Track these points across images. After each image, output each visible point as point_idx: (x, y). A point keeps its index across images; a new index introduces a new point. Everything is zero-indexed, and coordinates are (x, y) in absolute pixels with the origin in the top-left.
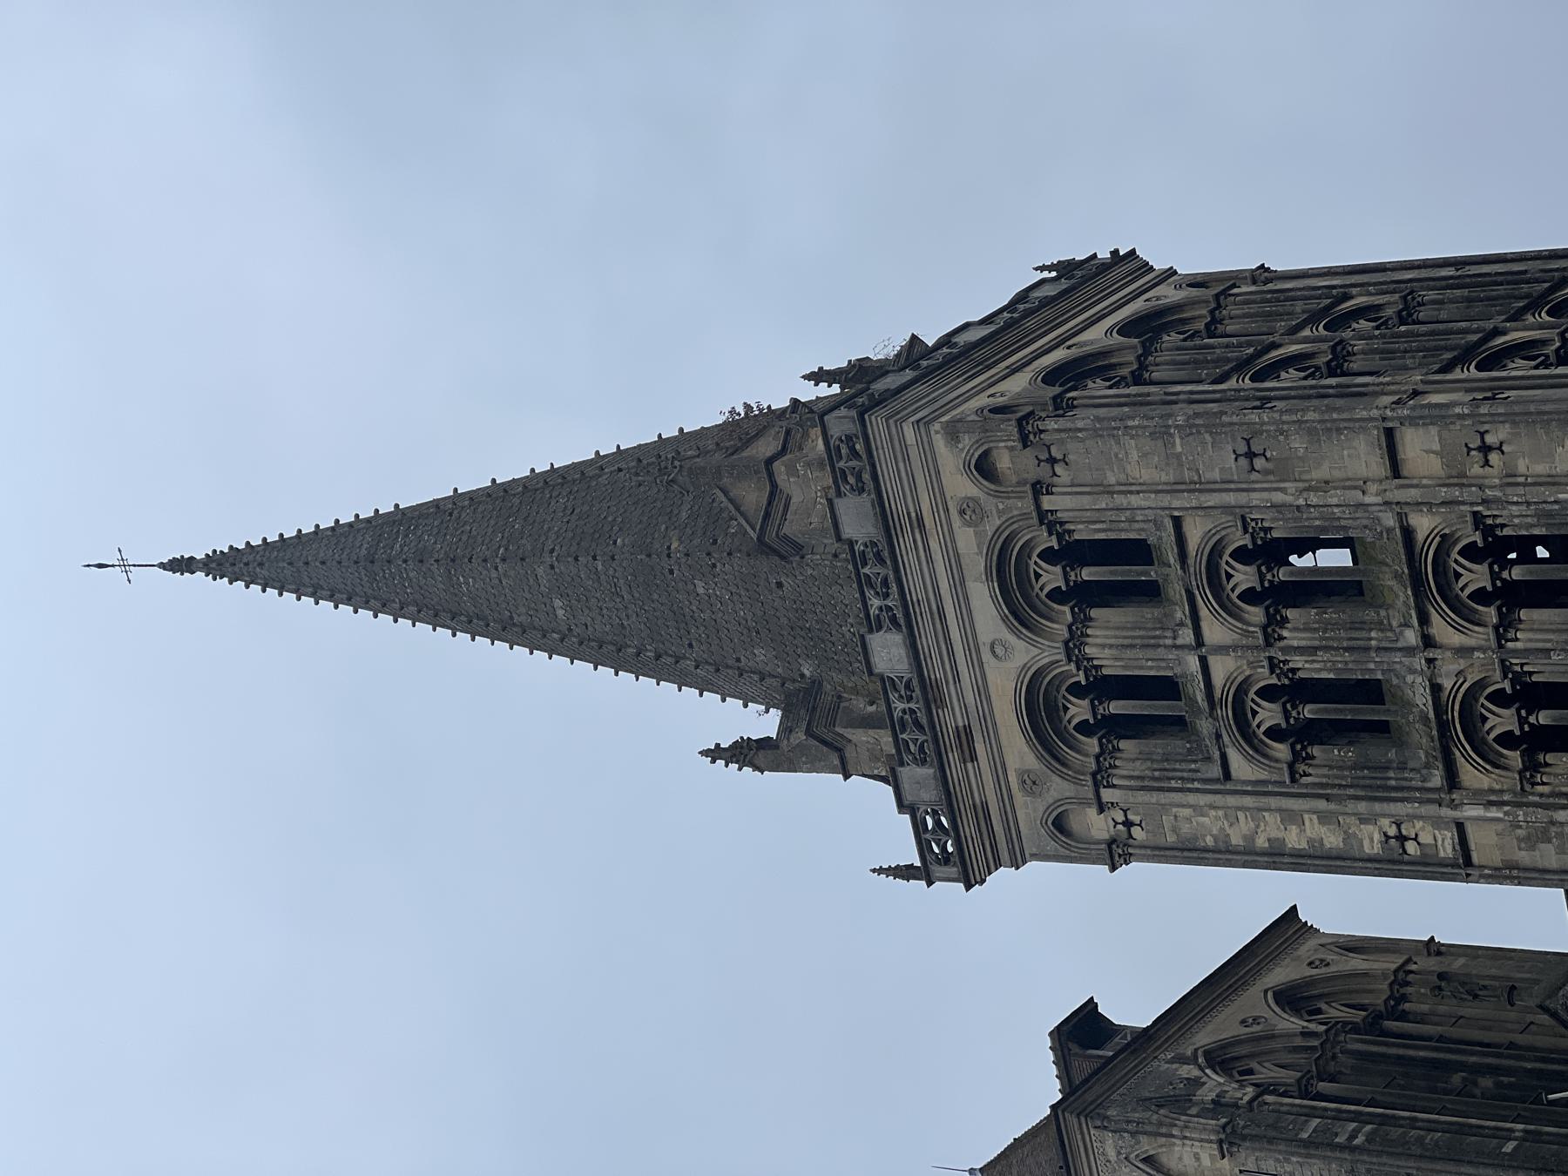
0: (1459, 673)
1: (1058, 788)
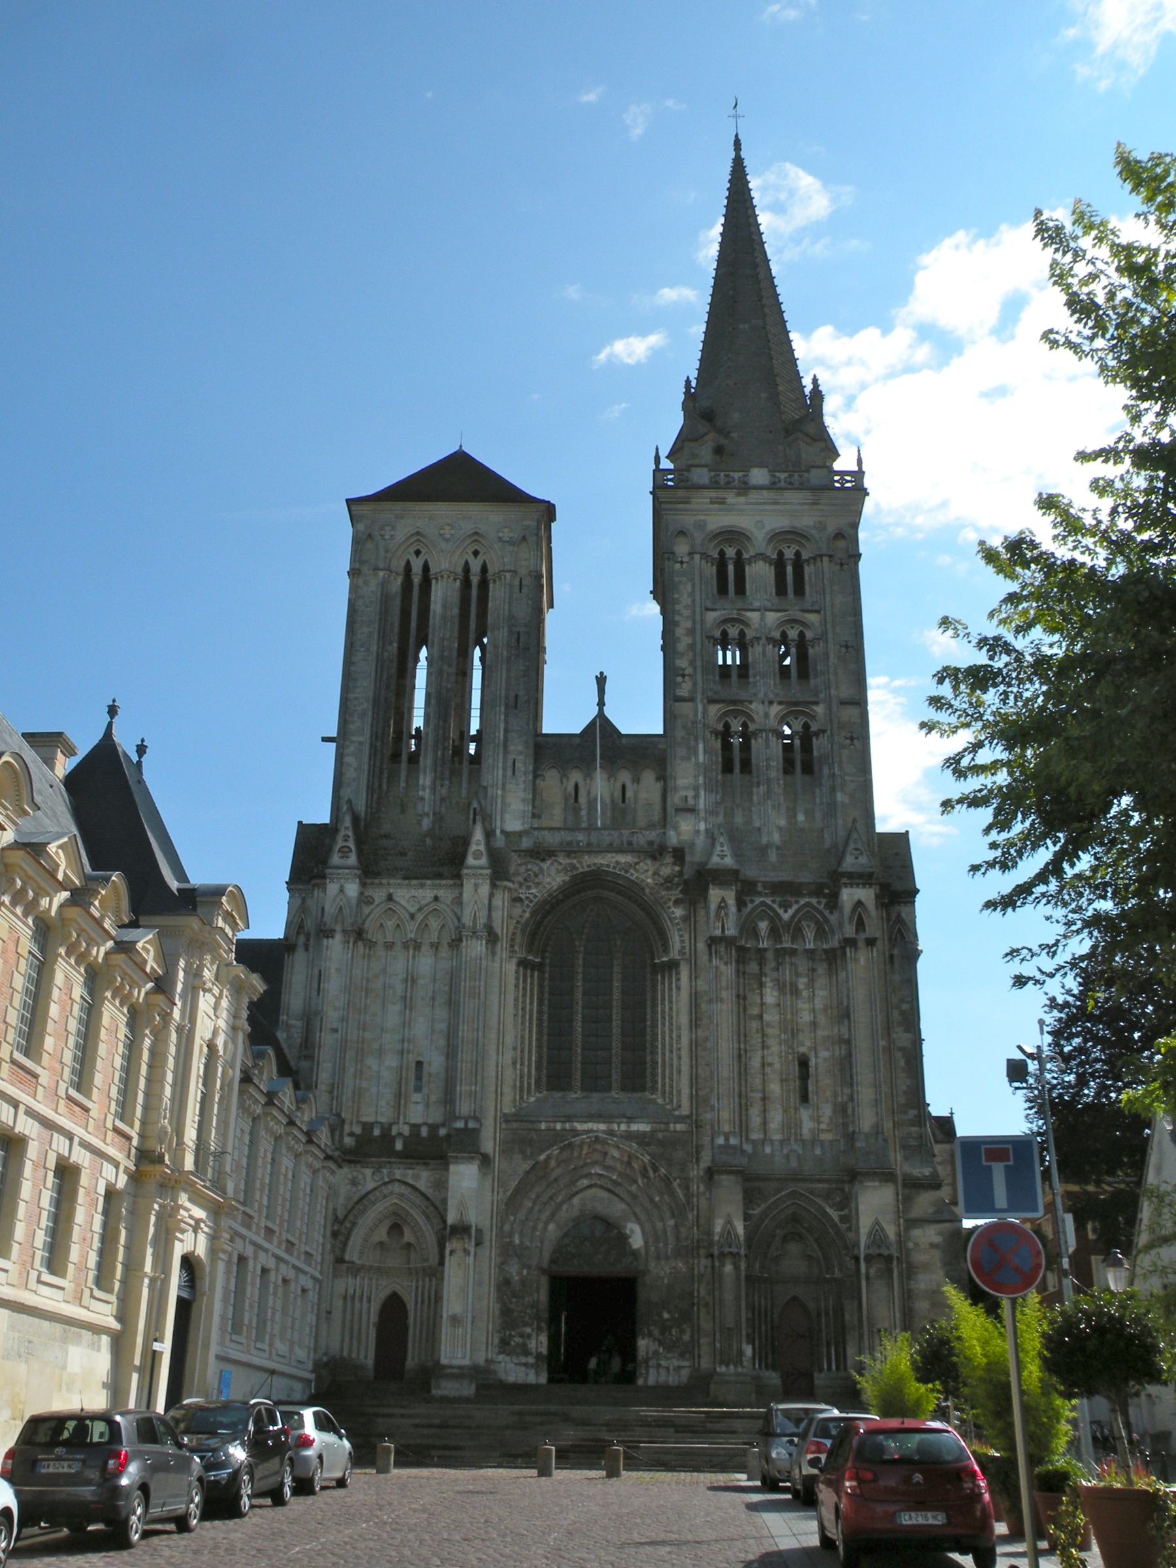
1: (699, 537)
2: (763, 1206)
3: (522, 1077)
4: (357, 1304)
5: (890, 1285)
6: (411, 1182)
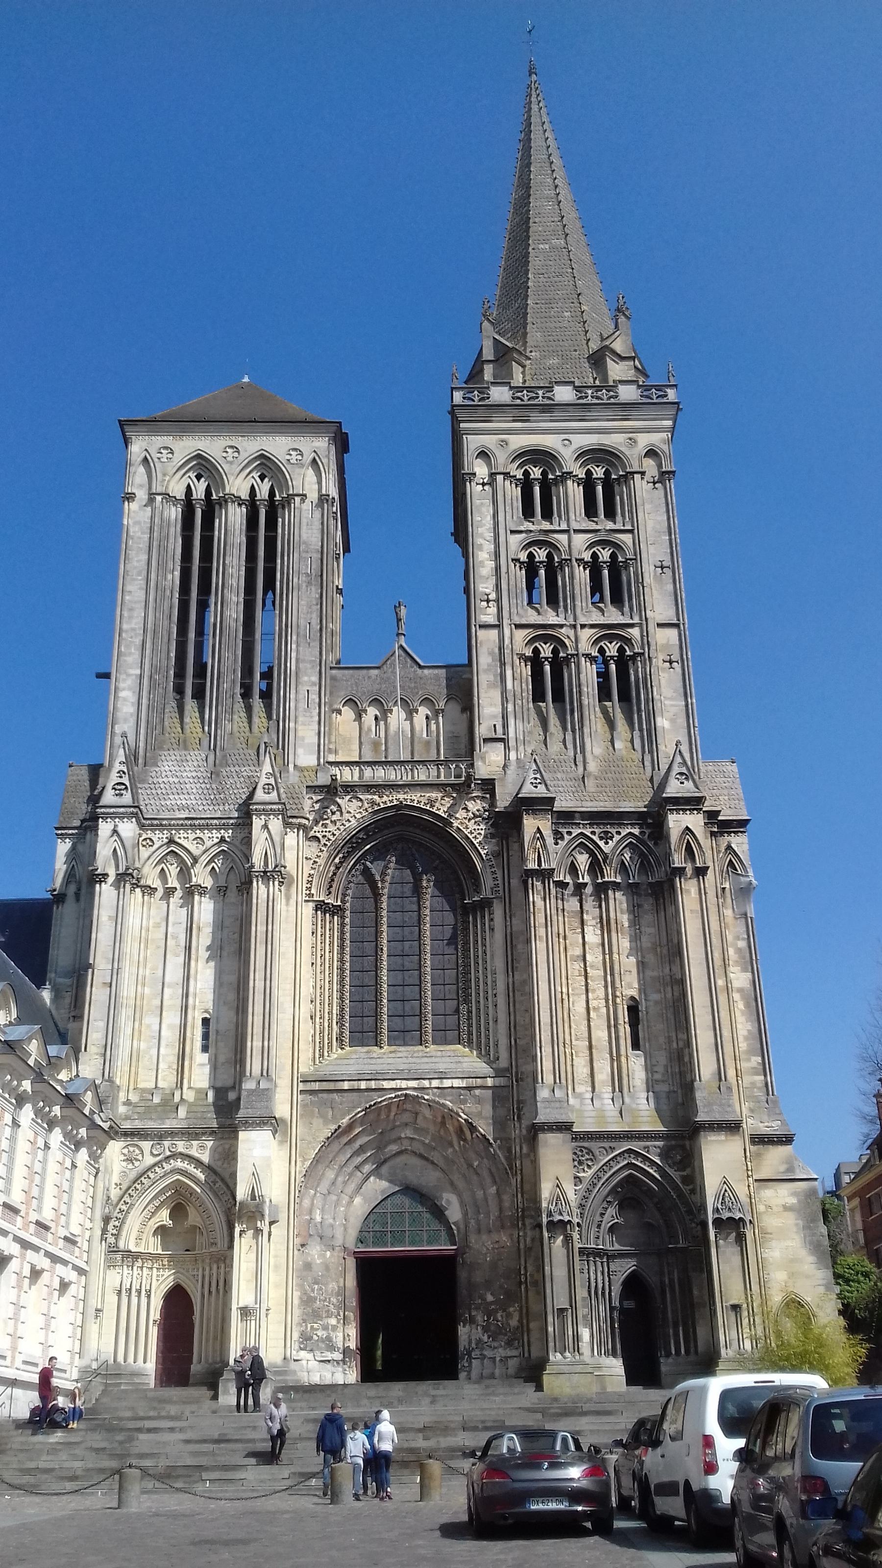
0: (569, 637)
2: (595, 1168)
3: (322, 1032)
4: (134, 1300)
5: (744, 1254)
6: (196, 1155)
